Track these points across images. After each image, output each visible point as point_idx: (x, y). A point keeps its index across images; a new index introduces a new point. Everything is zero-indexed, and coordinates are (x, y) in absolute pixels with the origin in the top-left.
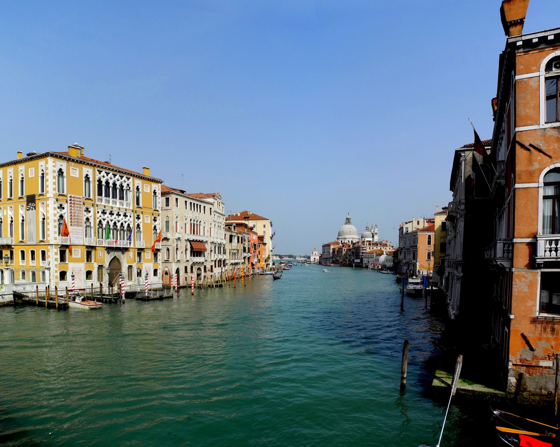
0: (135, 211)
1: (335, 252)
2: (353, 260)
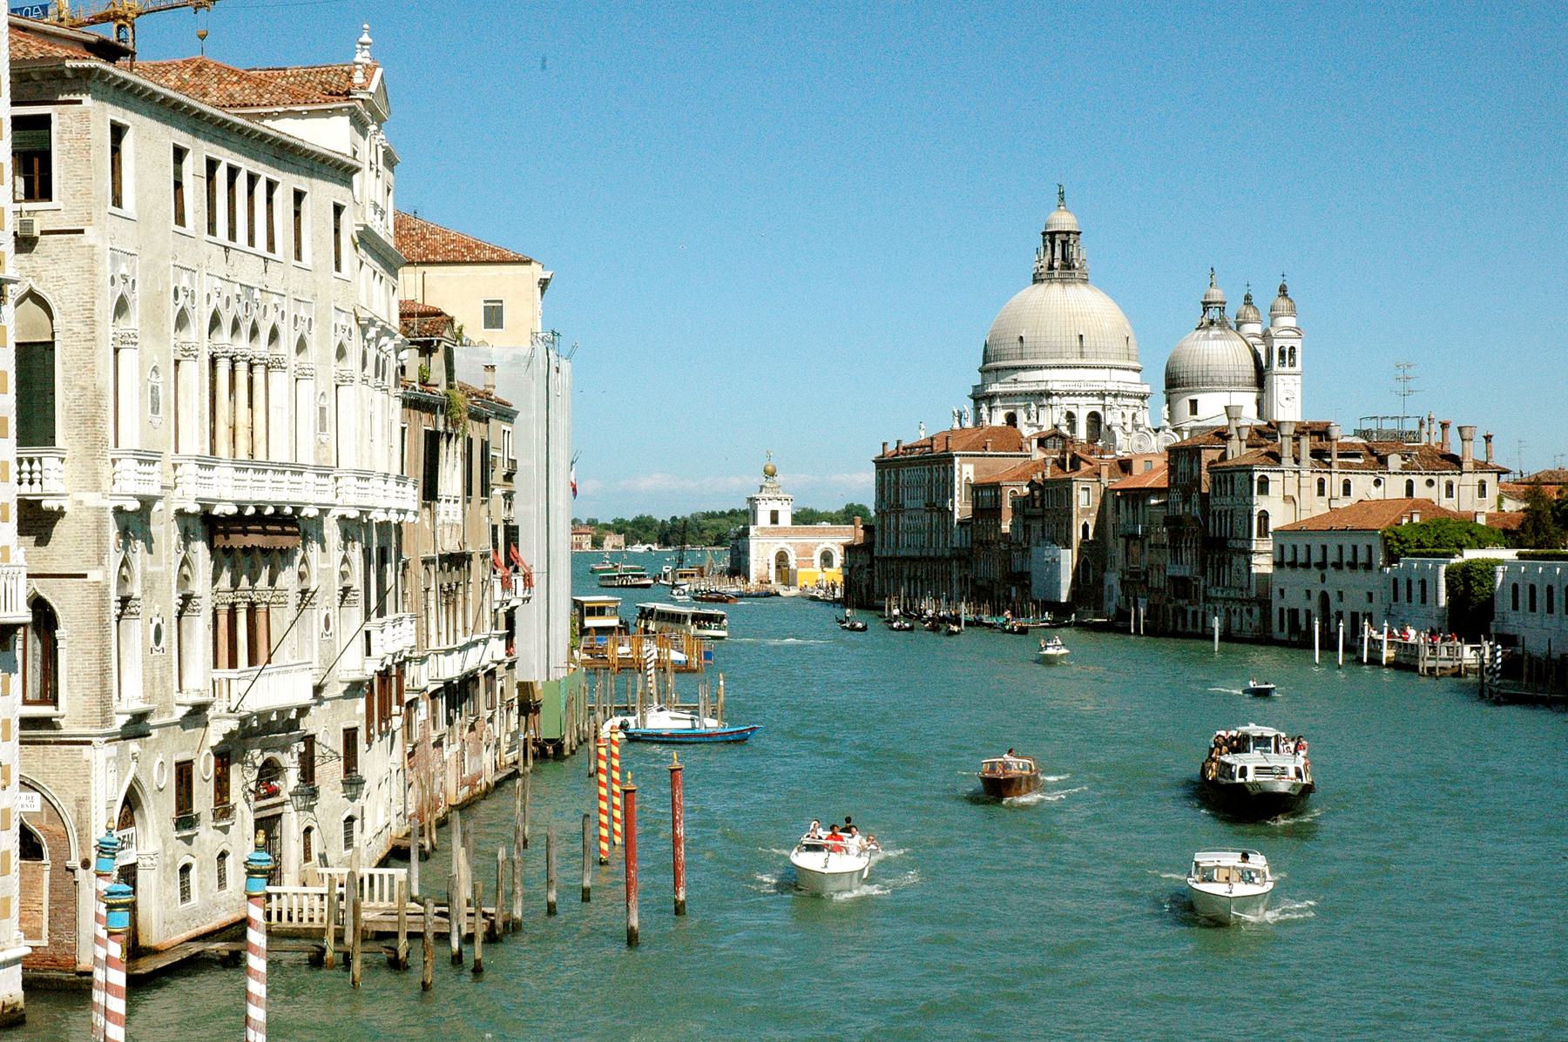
1: (996, 512)
2: (1173, 579)
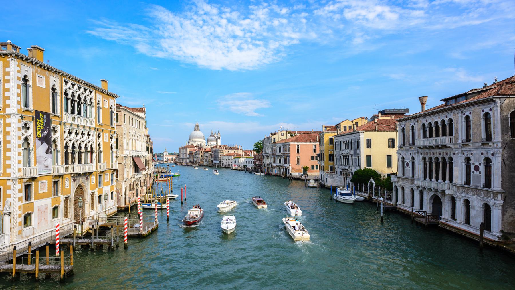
0: (97, 129)
2: (211, 161)
